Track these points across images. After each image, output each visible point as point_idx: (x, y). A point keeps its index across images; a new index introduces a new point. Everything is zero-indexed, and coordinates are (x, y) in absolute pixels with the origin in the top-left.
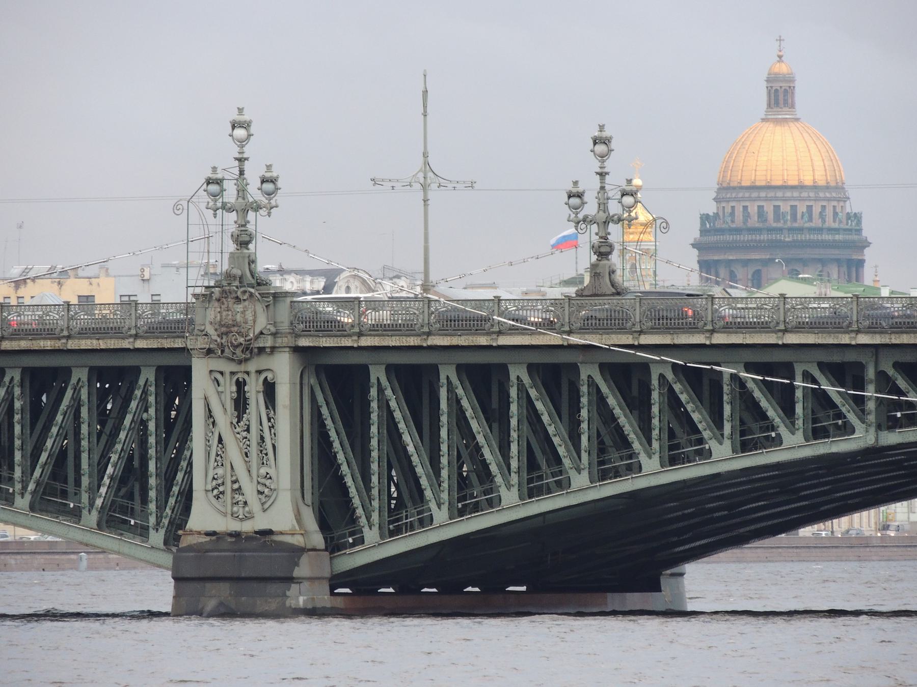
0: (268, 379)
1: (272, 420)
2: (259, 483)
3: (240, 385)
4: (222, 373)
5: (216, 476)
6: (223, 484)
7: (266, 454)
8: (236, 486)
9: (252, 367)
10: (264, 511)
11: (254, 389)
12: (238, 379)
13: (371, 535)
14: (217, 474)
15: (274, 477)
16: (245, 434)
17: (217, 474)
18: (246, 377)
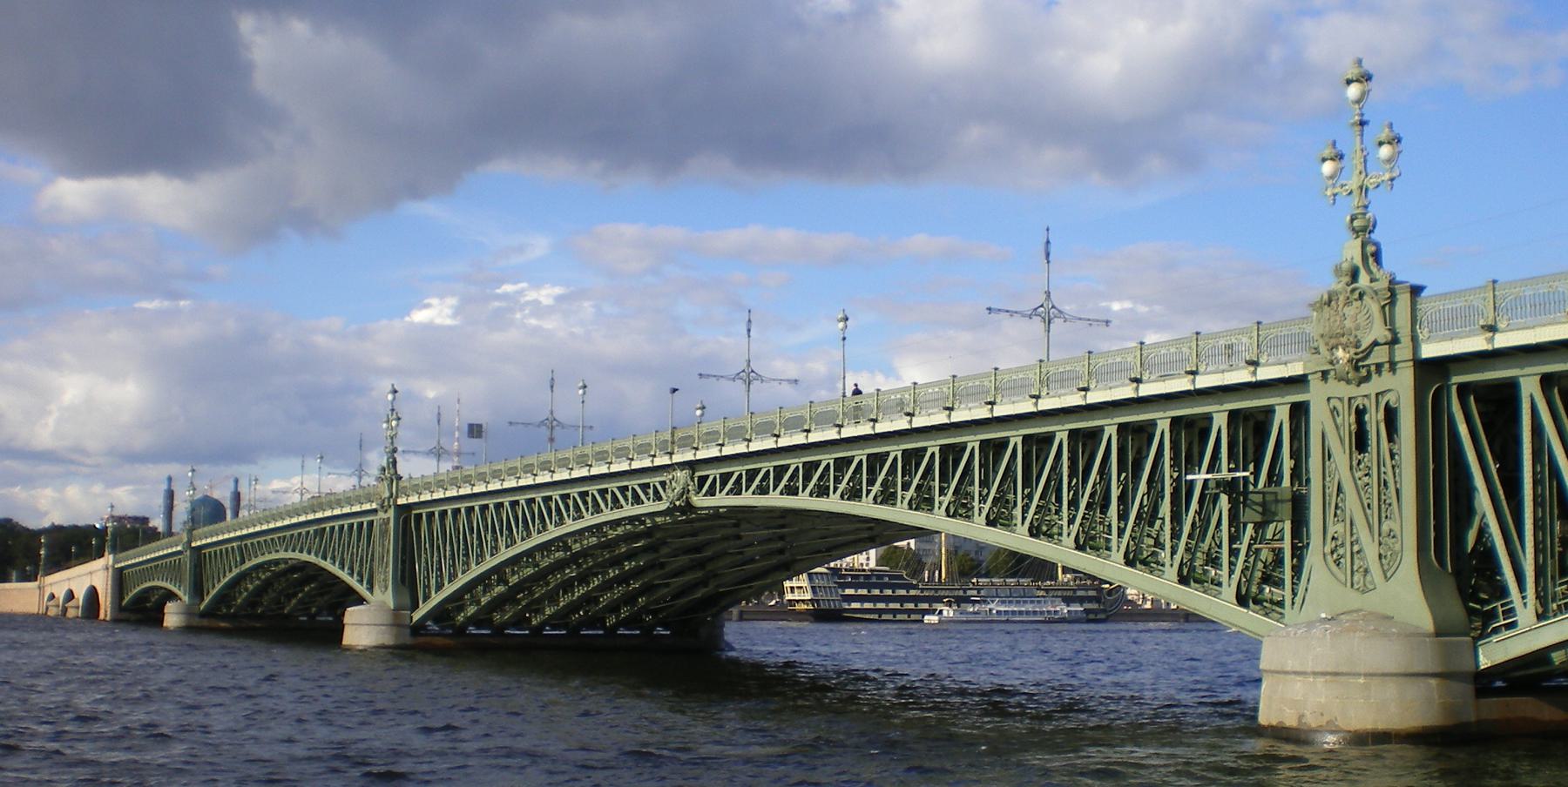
0: (1391, 403)
1: (1396, 457)
2: (1380, 544)
3: (1360, 413)
4: (1340, 399)
5: (1336, 535)
6: (1343, 545)
7: (1390, 505)
8: (1356, 548)
9: (1370, 388)
10: (1387, 579)
11: (1374, 419)
12: (1357, 407)
13: (1525, 613)
14: (1336, 532)
15: (1398, 534)
16: (1366, 479)
17: (1336, 532)
18: (1366, 402)
